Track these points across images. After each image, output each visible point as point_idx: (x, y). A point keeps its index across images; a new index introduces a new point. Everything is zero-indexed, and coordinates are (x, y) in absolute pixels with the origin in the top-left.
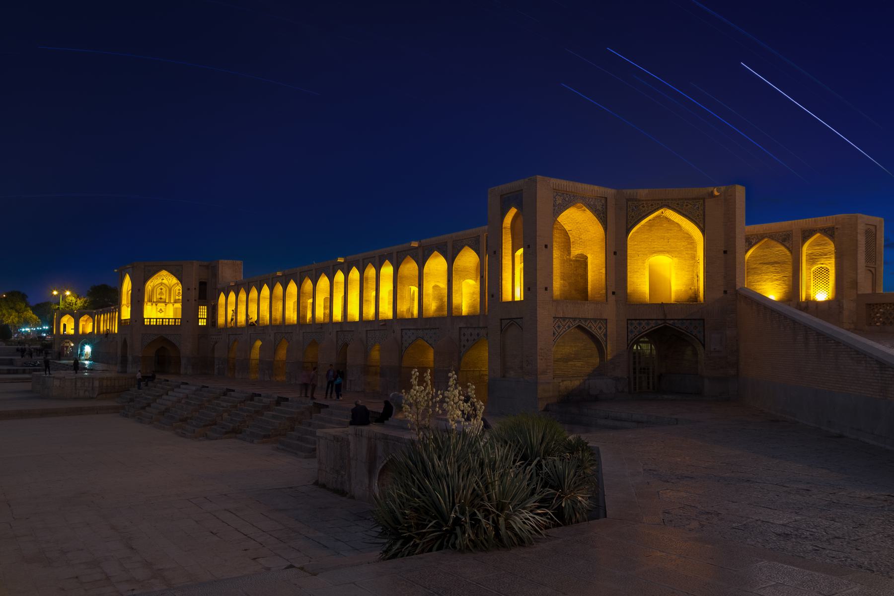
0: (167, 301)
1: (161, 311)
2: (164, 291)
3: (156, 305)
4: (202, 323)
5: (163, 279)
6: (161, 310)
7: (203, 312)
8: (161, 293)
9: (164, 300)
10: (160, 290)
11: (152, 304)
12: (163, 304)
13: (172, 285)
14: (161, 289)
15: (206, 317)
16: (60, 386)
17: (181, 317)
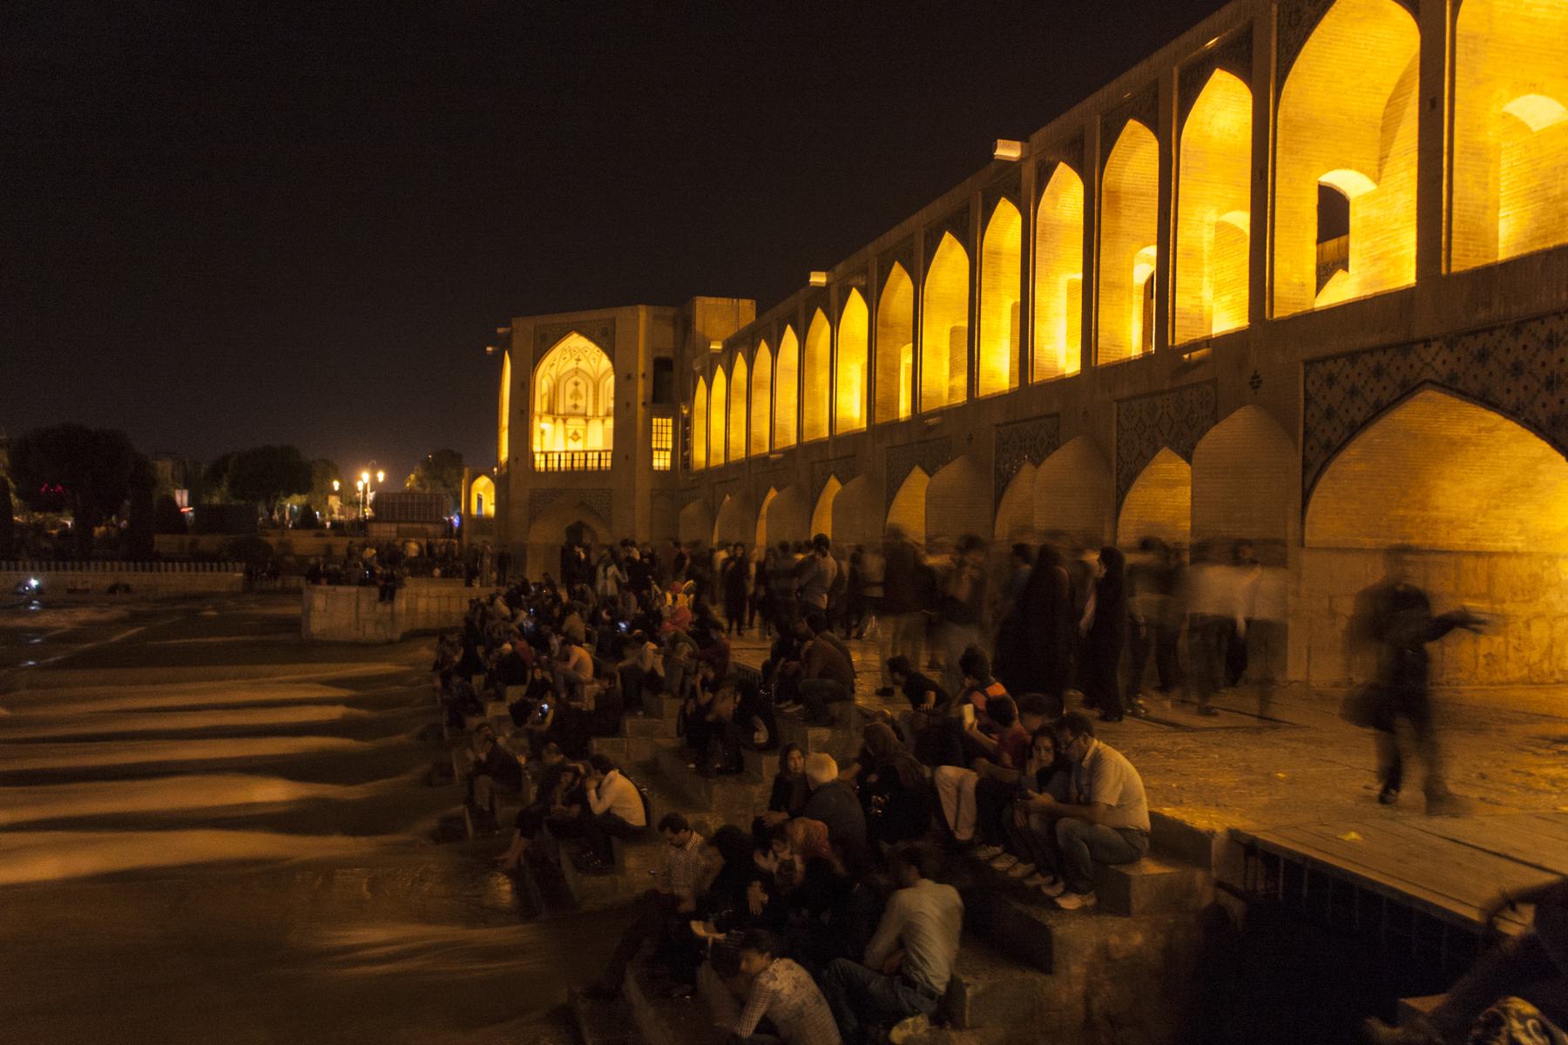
0: (590, 413)
1: (575, 437)
2: (582, 388)
3: (565, 421)
4: (662, 461)
5: (578, 360)
6: (575, 433)
7: (663, 432)
8: (576, 394)
9: (583, 412)
10: (574, 387)
11: (555, 420)
12: (581, 421)
13: (601, 373)
14: (576, 384)
15: (670, 446)
16: (325, 611)
17: (611, 448)
